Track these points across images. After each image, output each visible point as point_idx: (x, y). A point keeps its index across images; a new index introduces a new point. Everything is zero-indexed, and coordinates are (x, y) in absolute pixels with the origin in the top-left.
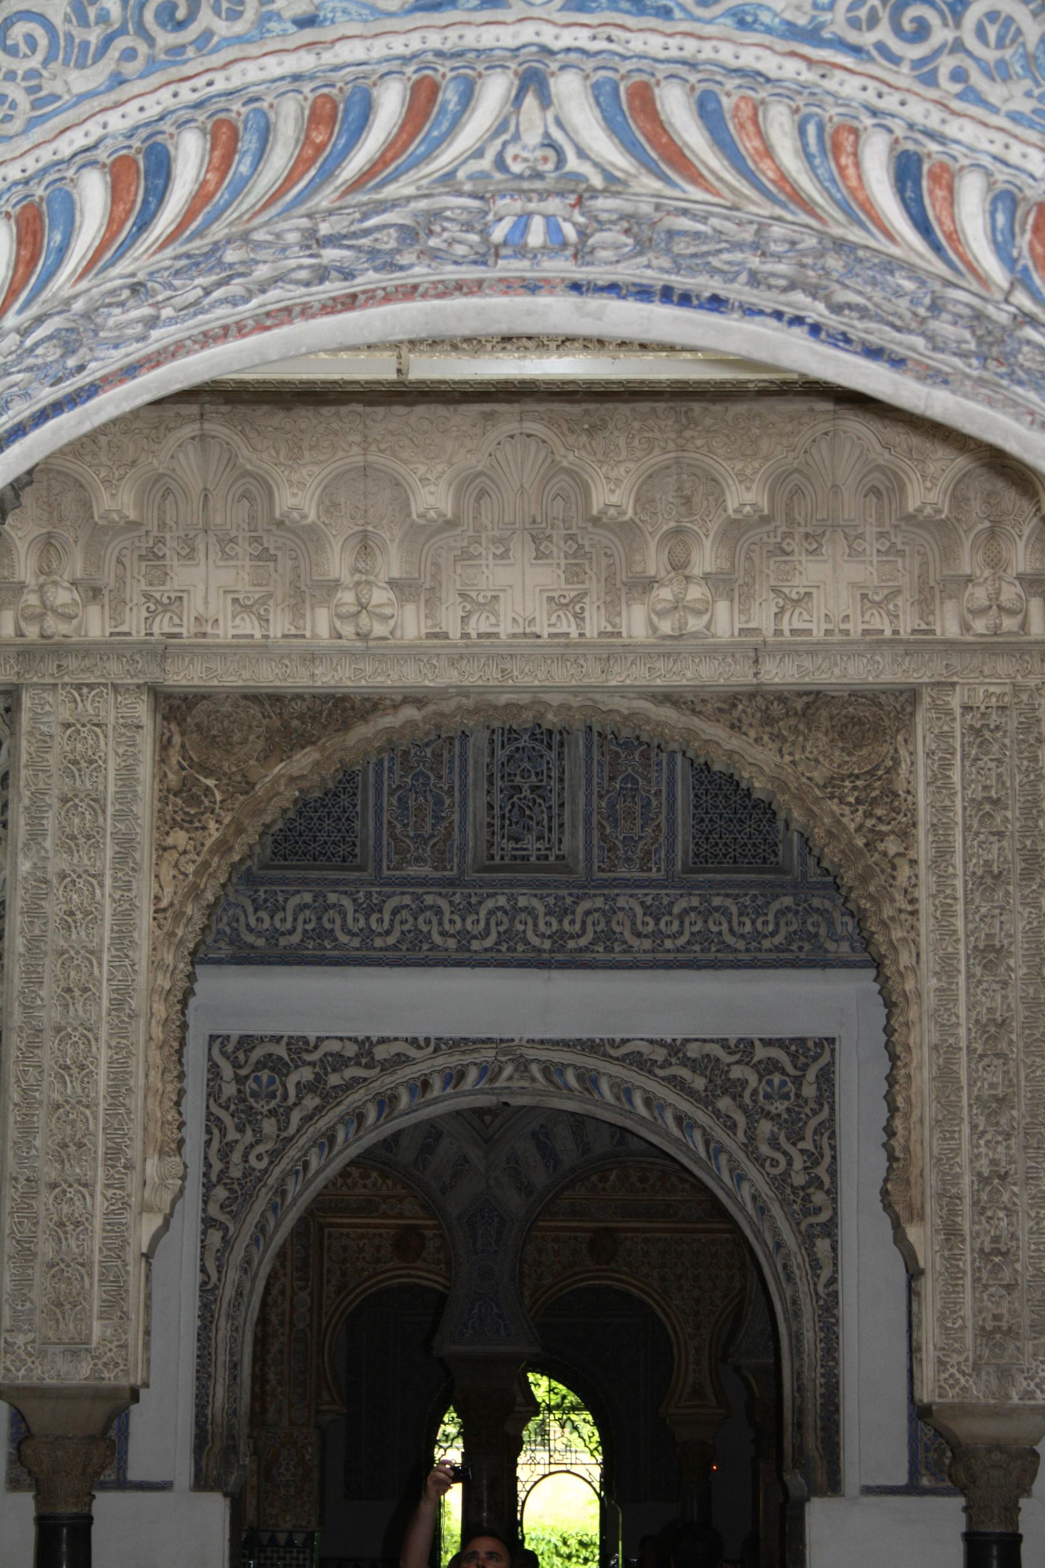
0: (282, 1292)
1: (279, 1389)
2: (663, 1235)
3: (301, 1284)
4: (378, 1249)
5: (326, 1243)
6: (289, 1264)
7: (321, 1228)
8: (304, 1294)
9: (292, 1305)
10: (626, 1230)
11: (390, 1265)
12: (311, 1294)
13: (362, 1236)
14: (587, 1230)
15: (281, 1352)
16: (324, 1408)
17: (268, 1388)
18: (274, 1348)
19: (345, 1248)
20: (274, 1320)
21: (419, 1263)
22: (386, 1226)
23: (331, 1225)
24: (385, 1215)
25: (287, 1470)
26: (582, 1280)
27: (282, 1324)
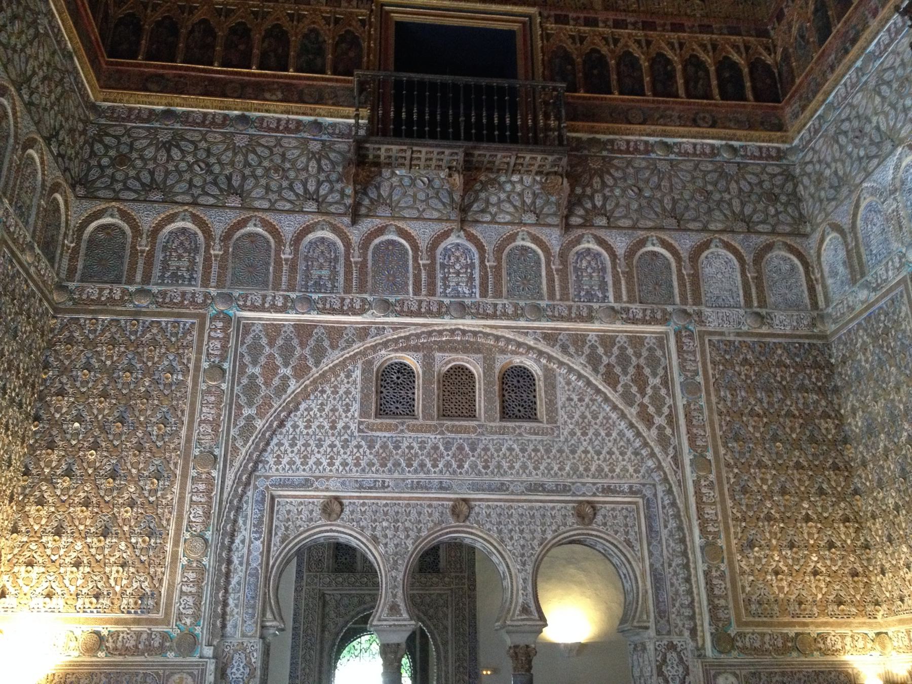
0: (243, 542)
1: (236, 610)
2: (499, 504)
3: (257, 536)
4: (311, 512)
5: (276, 508)
6: (249, 522)
7: (273, 498)
8: (258, 543)
9: (249, 550)
10: (475, 500)
11: (319, 523)
12: (263, 543)
13: (301, 503)
14: (450, 500)
15: (239, 583)
16: (268, 624)
17: (228, 610)
18: (234, 581)
19: (289, 512)
20: (236, 561)
21: (339, 522)
22: (317, 497)
23: (280, 496)
24: (317, 489)
25: (238, 670)
26: (447, 533)
27: (241, 564)
